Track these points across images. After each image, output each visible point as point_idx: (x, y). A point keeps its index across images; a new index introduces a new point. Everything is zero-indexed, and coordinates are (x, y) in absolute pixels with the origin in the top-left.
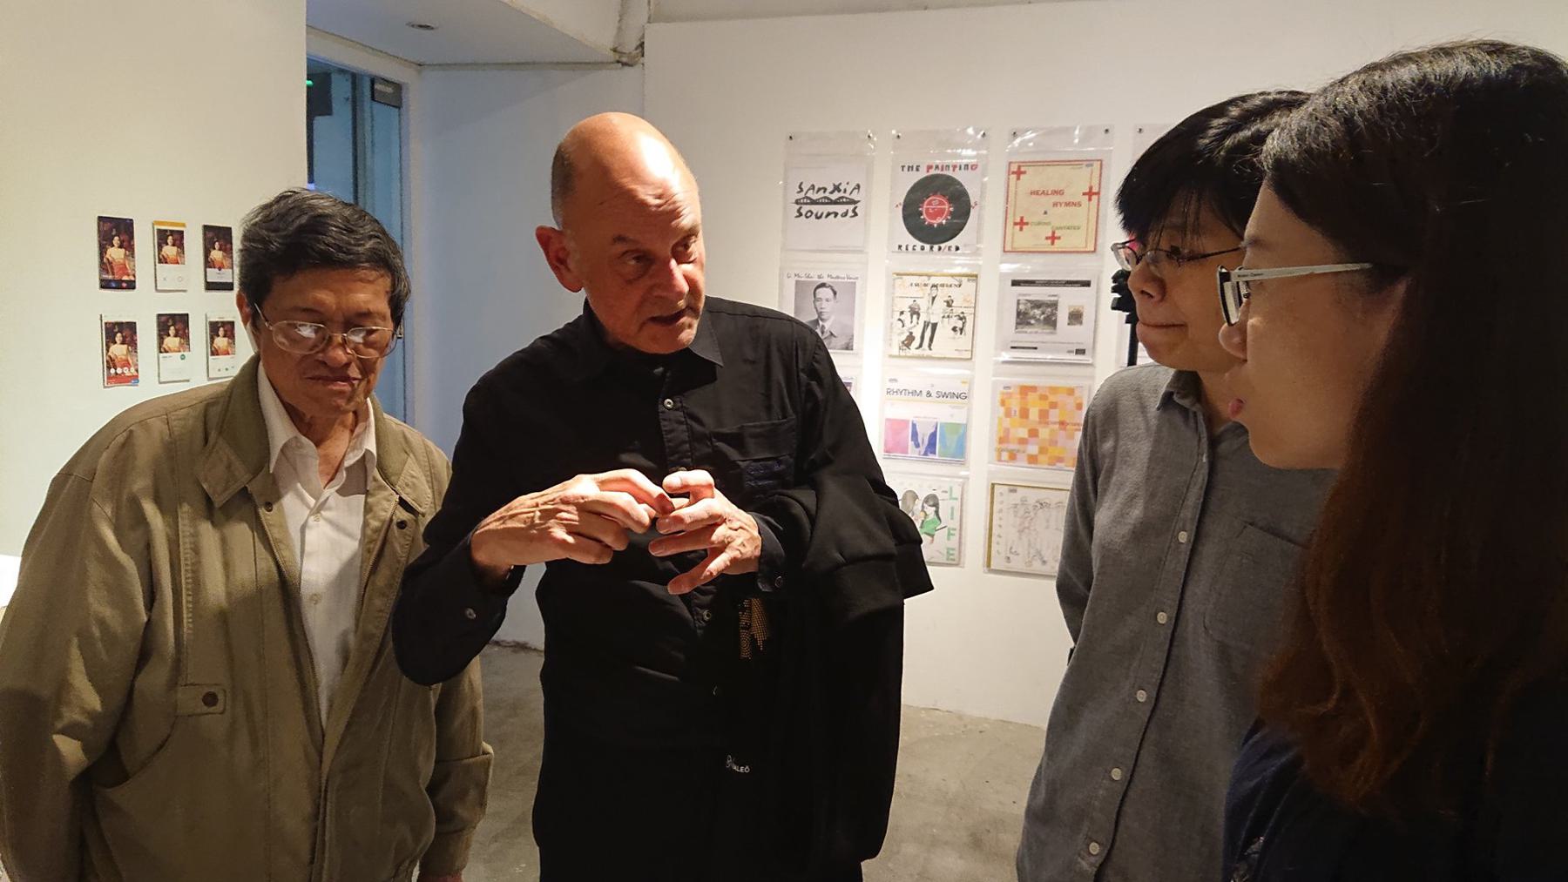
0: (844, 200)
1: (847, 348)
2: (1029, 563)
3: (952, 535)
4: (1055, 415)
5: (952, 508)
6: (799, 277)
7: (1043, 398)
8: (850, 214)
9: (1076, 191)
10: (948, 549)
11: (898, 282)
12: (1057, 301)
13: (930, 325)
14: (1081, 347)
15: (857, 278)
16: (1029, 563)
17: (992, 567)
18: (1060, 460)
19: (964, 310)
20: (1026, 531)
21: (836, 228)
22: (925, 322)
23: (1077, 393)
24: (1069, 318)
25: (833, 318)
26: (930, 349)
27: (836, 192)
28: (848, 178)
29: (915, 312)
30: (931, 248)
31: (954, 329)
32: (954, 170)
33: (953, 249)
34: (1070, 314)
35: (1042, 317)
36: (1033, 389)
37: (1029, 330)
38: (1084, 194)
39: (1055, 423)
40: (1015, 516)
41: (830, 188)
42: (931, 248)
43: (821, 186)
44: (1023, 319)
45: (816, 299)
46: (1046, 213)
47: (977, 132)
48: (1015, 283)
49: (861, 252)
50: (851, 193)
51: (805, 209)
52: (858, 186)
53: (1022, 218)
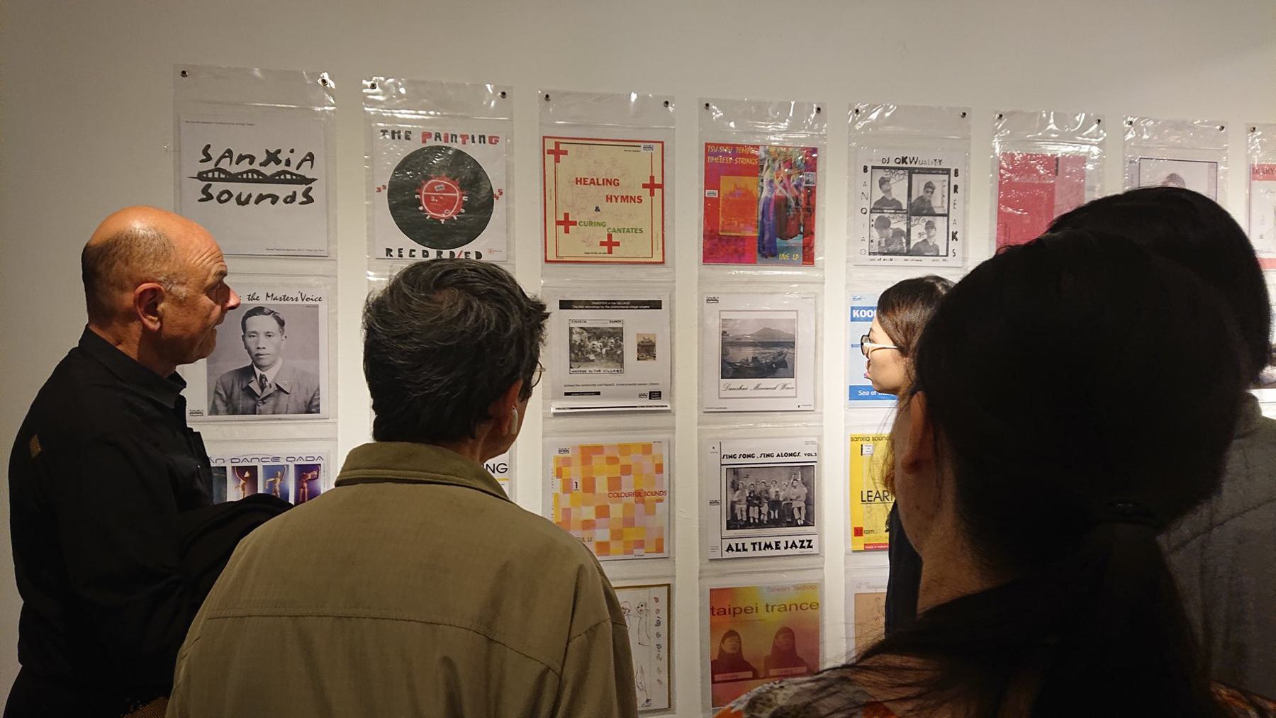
0: (288, 177)
1: (309, 412)
4: (628, 484)
7: (612, 460)
8: (300, 198)
9: (633, 183)
12: (622, 329)
15: (320, 299)
18: (640, 544)
23: (655, 451)
32: (464, 143)
34: (639, 345)
35: (604, 350)
36: (598, 449)
37: (588, 370)
38: (645, 186)
39: (630, 494)
41: (262, 157)
44: (578, 354)
46: (597, 209)
47: (495, 91)
50: (298, 168)
51: (216, 188)
52: (311, 157)
53: (566, 215)
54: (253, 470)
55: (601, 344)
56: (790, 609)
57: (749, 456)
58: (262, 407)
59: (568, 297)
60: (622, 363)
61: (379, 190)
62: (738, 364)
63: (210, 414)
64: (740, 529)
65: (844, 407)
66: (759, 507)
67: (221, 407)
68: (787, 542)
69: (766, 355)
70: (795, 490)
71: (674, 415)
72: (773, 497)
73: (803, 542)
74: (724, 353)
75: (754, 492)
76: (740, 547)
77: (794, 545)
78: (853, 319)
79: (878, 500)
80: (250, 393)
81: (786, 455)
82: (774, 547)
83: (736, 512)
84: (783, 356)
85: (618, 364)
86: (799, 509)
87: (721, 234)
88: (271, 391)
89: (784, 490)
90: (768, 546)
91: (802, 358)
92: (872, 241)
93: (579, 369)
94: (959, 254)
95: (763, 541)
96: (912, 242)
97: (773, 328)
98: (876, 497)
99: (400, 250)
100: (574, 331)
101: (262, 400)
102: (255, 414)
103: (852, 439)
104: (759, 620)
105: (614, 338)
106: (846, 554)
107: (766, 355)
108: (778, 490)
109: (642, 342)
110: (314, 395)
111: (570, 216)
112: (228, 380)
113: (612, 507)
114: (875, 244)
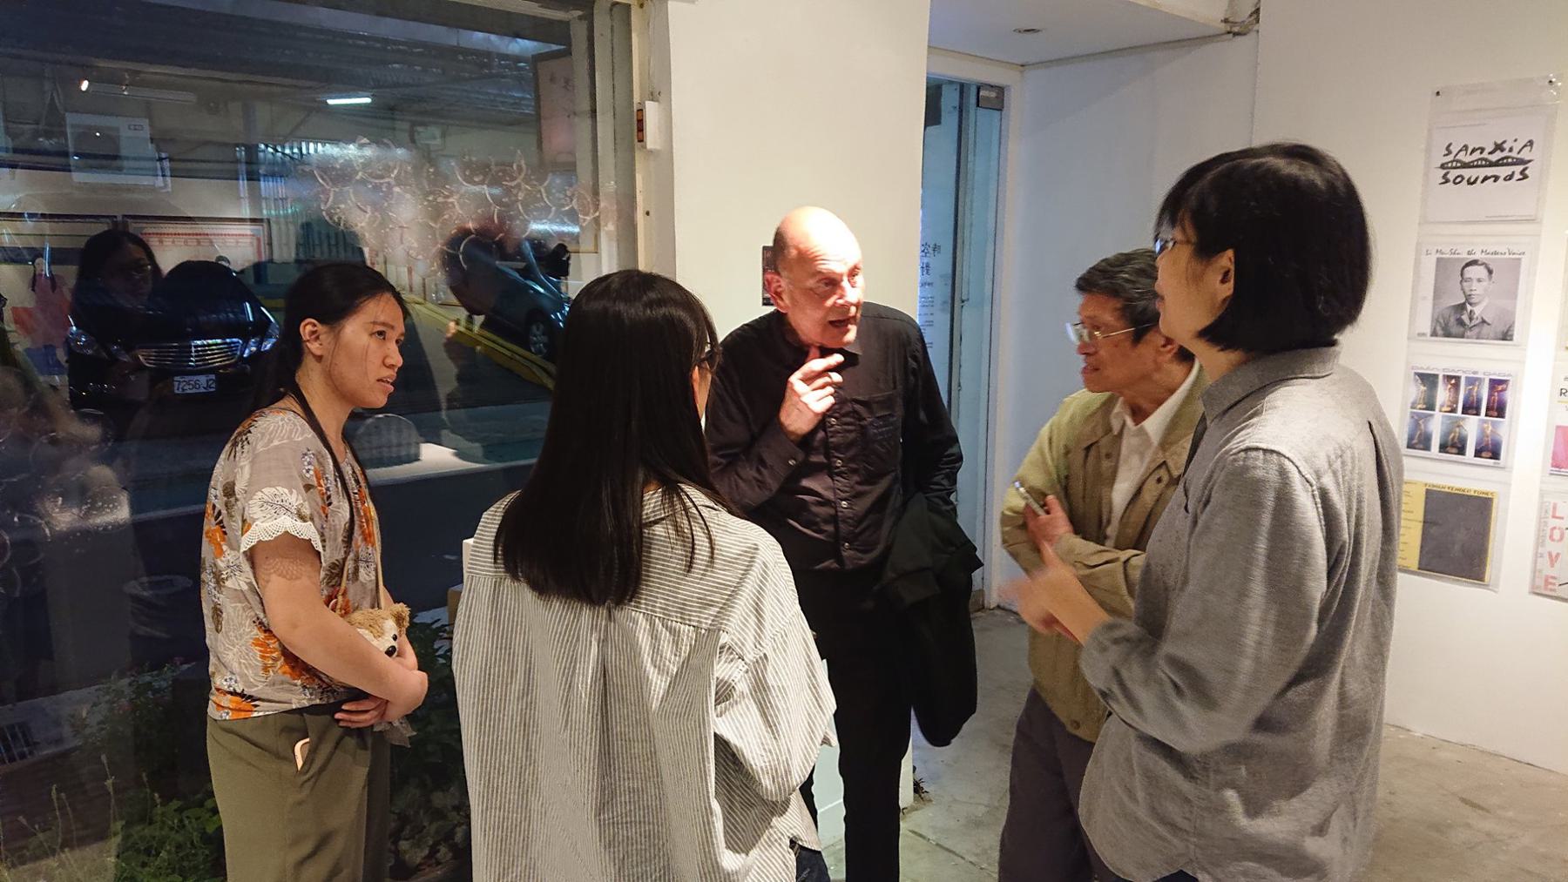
0: (1510, 160)
1: (1504, 339)
8: (1517, 176)
21: (1496, 195)
25: (1484, 304)
27: (1498, 152)
28: (1513, 133)
43: (1477, 147)
45: (1463, 279)
49: (1531, 220)
50: (1519, 153)
51: (1453, 174)
52: (1531, 143)
54: (1458, 378)
58: (1468, 333)
63: (1432, 335)
67: (1440, 331)
80: (1461, 323)
88: (1478, 322)
110: (1510, 327)
112: (1447, 313)
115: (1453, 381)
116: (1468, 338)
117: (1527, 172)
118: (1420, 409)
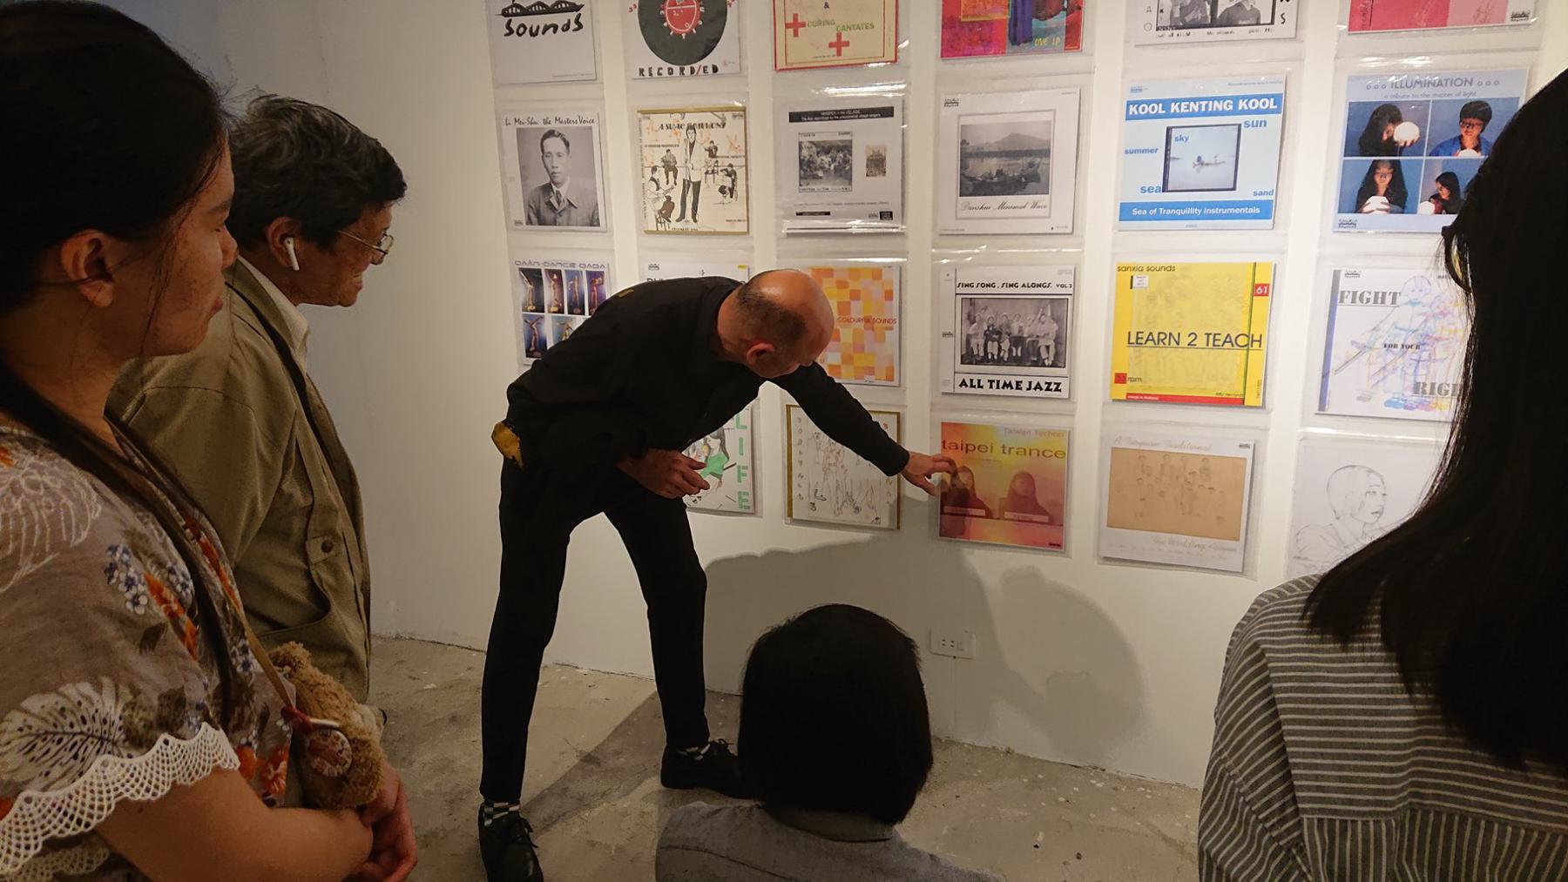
0: (564, 5)
1: (592, 225)
2: (839, 511)
3: (745, 475)
4: (857, 310)
5: (741, 440)
6: (520, 123)
7: (842, 285)
8: (573, 26)
10: (740, 492)
11: (645, 123)
12: (851, 141)
13: (691, 185)
14: (885, 208)
16: (839, 511)
17: (794, 517)
18: (871, 371)
19: (731, 161)
20: (833, 468)
22: (684, 180)
24: (867, 166)
26: (695, 221)
29: (670, 167)
30: (682, 70)
31: (722, 190)
33: (710, 70)
34: (868, 160)
35: (832, 166)
37: (816, 187)
39: (859, 320)
40: (818, 450)
42: (682, 70)
44: (808, 170)
46: (827, 6)
48: (795, 117)
51: (516, 22)
53: (795, 16)
54: (559, 273)
55: (830, 160)
56: (1030, 454)
57: (988, 285)
58: (559, 220)
59: (798, 109)
60: (851, 180)
61: (631, 10)
62: (980, 179)
64: (976, 364)
65: (1113, 230)
66: (999, 343)
67: (534, 219)
68: (1030, 383)
69: (1013, 167)
70: (1043, 326)
71: (907, 238)
72: (1015, 332)
73: (1050, 384)
74: (963, 166)
75: (993, 325)
76: (975, 383)
77: (1038, 387)
78: (1129, 118)
79: (1150, 343)
81: (1034, 285)
82: (1014, 386)
83: (971, 346)
84: (1036, 167)
85: (847, 181)
86: (1048, 347)
87: (963, 20)
89: (1030, 326)
90: (1010, 385)
91: (1059, 168)
92: (1162, 11)
93: (808, 187)
94: (1291, 19)
95: (1002, 380)
96: (1219, 8)
97: (1023, 134)
98: (1147, 340)
99: (650, 69)
100: (803, 146)
101: (560, 213)
102: (555, 225)
103: (1119, 269)
104: (994, 461)
105: (842, 151)
106: (1104, 403)
107: (1013, 167)
108: (1021, 325)
109: (872, 156)
110: (593, 213)
111: (799, 17)
113: (841, 330)
114: (1166, 15)
115: (555, 274)
116: (559, 225)
117: (580, 20)
118: (532, 311)
